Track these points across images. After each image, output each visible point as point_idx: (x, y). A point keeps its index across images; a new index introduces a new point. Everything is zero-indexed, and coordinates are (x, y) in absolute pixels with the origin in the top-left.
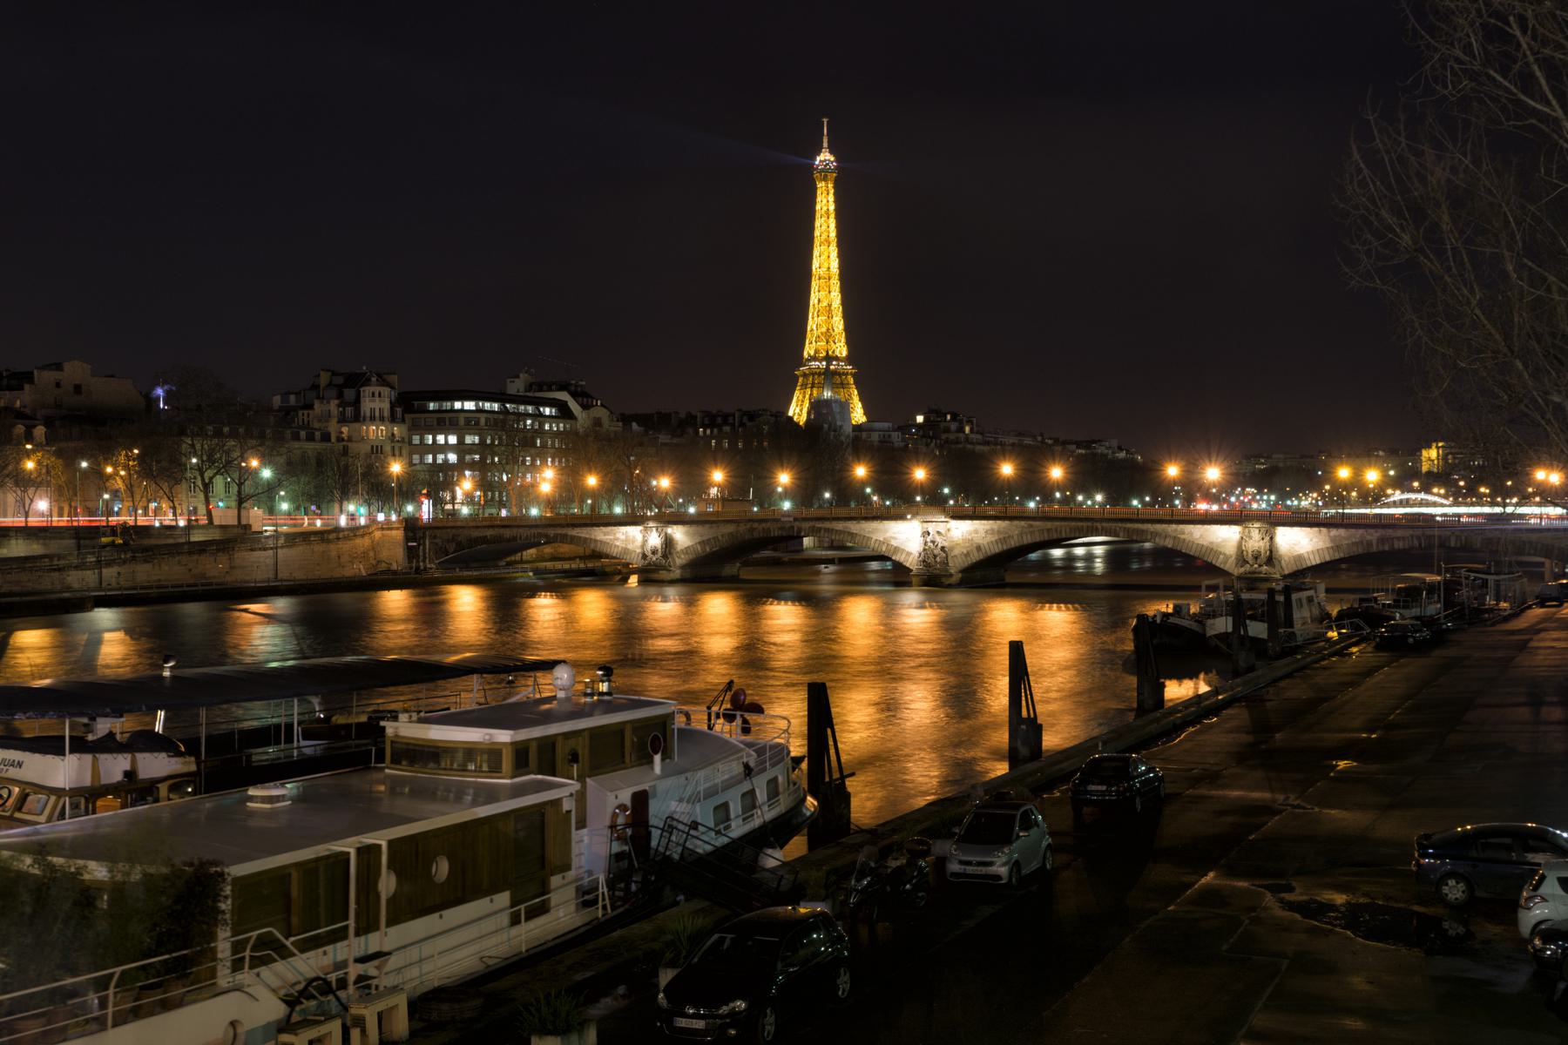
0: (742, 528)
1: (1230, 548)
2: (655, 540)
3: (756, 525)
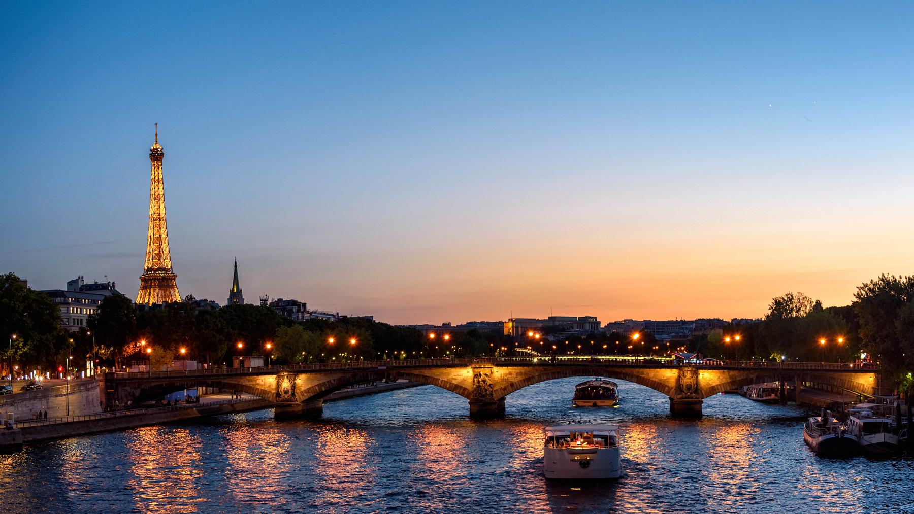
1: (672, 383)
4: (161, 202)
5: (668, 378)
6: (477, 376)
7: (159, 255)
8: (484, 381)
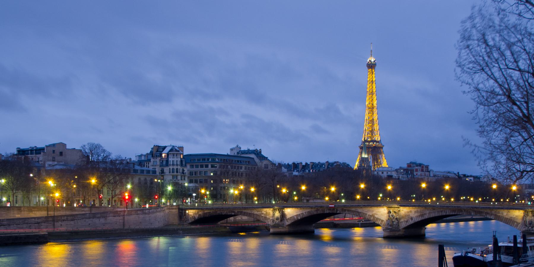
0: (313, 210)
1: (520, 220)
2: (277, 214)
4: (374, 96)
5: (517, 216)
7: (372, 132)
8: (392, 216)
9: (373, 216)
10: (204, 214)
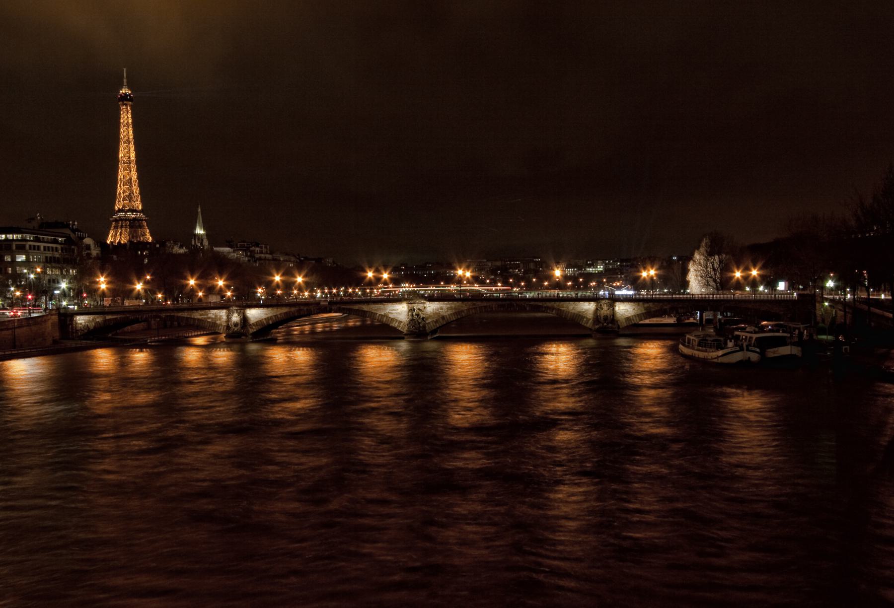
0: (293, 309)
1: (590, 315)
2: (235, 318)
3: (302, 307)
5: (586, 310)
6: (411, 310)
8: (418, 315)
9: (386, 316)
10: (105, 321)
